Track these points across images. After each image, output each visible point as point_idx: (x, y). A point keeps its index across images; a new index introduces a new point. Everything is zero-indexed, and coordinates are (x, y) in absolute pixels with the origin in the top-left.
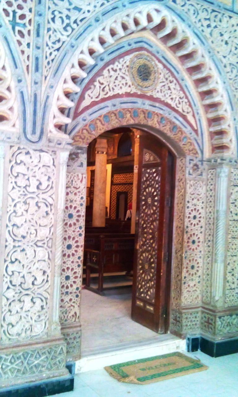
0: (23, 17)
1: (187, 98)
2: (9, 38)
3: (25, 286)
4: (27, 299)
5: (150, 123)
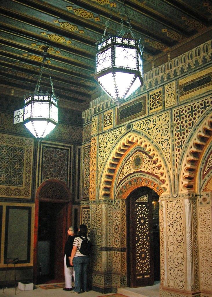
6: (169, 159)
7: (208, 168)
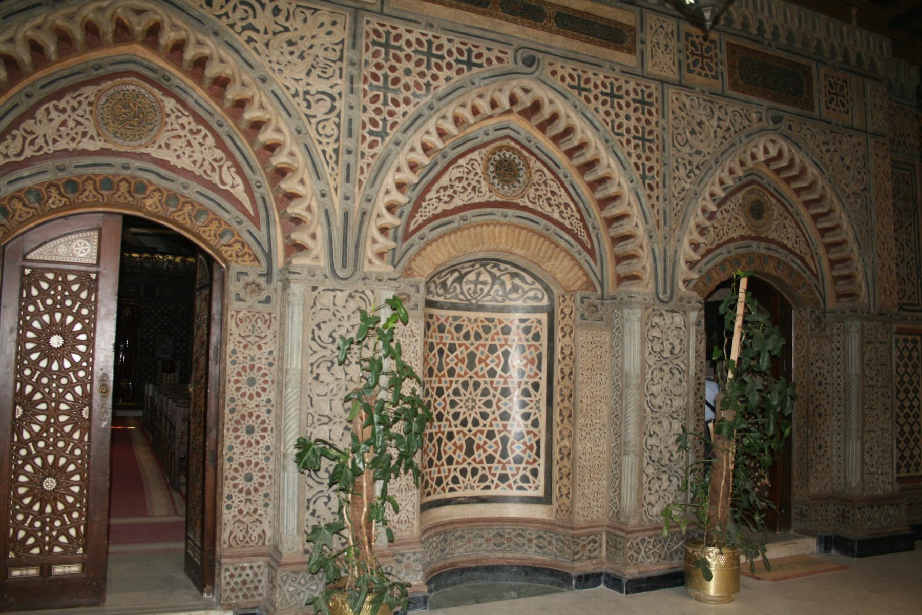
0: (651, 169)
1: (804, 236)
3: (663, 462)
4: (665, 477)
5: (766, 270)
6: (331, 157)
7: (424, 218)
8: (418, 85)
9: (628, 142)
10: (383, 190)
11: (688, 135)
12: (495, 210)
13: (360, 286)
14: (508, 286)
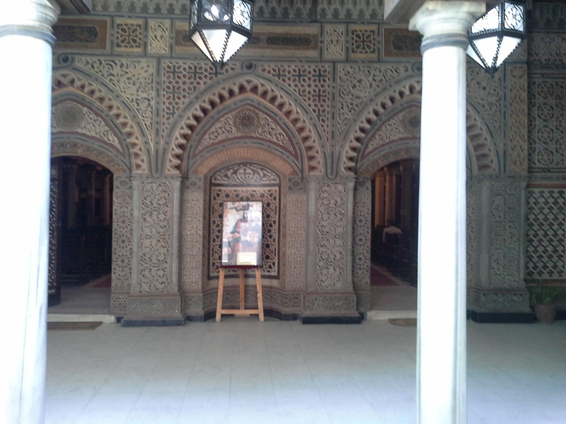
0: (324, 111)
2: (317, 125)
8: (189, 89)
9: (309, 99)
10: (174, 138)
11: (351, 89)
12: (240, 141)
13: (164, 180)
14: (261, 174)
